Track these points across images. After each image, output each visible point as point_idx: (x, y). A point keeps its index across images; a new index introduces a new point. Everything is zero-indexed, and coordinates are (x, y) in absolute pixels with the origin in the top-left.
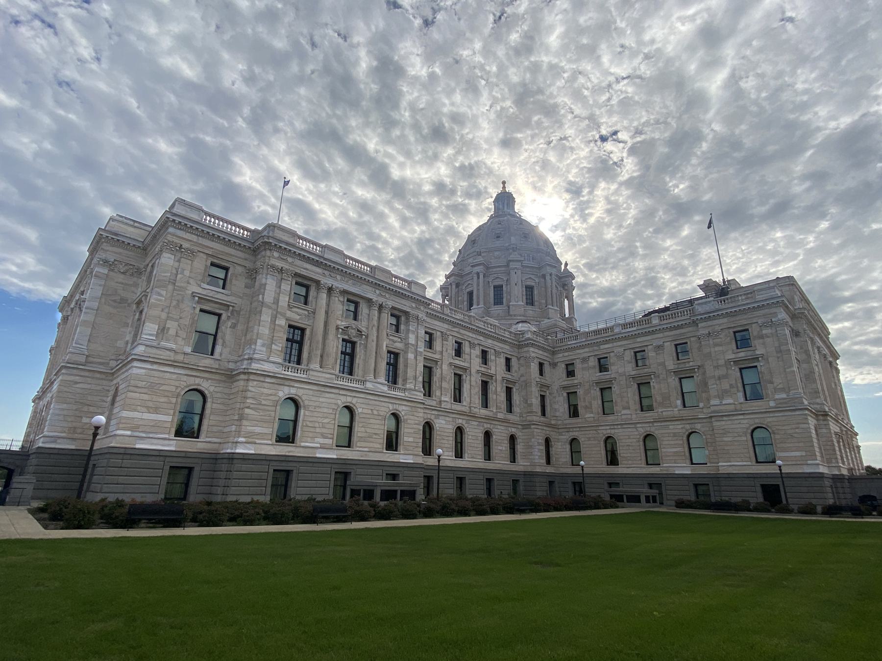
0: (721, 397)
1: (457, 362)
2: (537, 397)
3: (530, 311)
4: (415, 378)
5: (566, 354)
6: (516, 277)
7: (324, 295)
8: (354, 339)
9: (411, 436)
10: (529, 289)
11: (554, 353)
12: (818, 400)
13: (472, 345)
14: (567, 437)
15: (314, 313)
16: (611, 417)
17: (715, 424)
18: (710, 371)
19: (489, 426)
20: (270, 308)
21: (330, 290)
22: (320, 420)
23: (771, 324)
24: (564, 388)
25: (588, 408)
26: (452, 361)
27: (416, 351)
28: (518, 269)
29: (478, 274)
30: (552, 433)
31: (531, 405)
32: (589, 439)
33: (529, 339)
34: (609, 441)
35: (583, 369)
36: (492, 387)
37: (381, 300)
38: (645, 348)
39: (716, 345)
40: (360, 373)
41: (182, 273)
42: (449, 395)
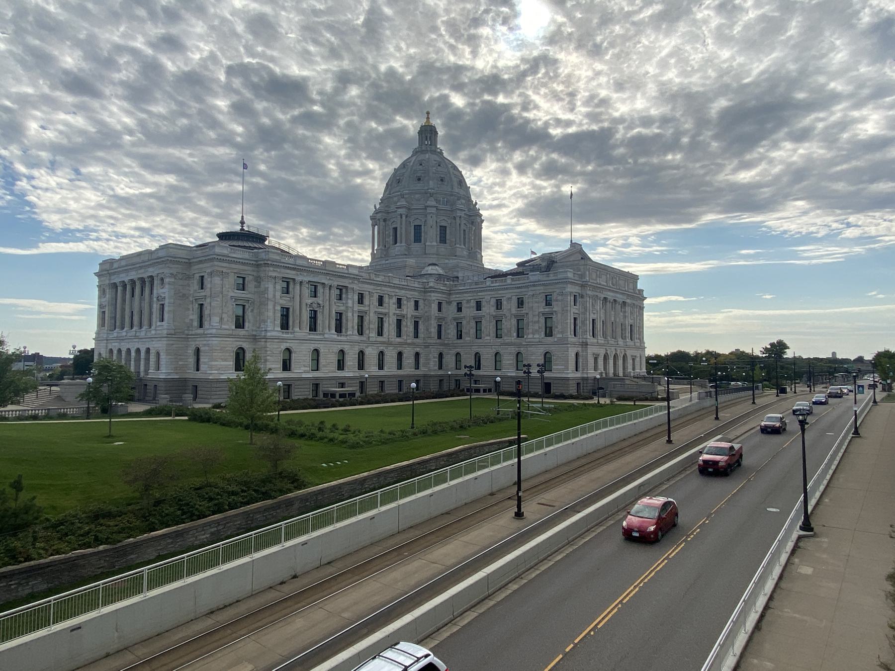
0: (534, 334)
1: (380, 310)
2: (435, 327)
3: (443, 248)
4: (353, 327)
5: (458, 296)
6: (431, 221)
7: (298, 287)
9: (351, 360)
10: (443, 229)
11: (450, 294)
12: (585, 337)
13: (390, 297)
14: (454, 352)
16: (480, 341)
18: (530, 316)
19: (401, 349)
20: (272, 301)
21: (301, 283)
22: (302, 358)
23: (562, 294)
24: (455, 319)
25: (468, 334)
26: (377, 310)
28: (433, 214)
29: (401, 215)
32: (466, 354)
33: (431, 287)
34: (478, 355)
35: (467, 307)
36: (404, 323)
39: (536, 302)
42: (374, 332)
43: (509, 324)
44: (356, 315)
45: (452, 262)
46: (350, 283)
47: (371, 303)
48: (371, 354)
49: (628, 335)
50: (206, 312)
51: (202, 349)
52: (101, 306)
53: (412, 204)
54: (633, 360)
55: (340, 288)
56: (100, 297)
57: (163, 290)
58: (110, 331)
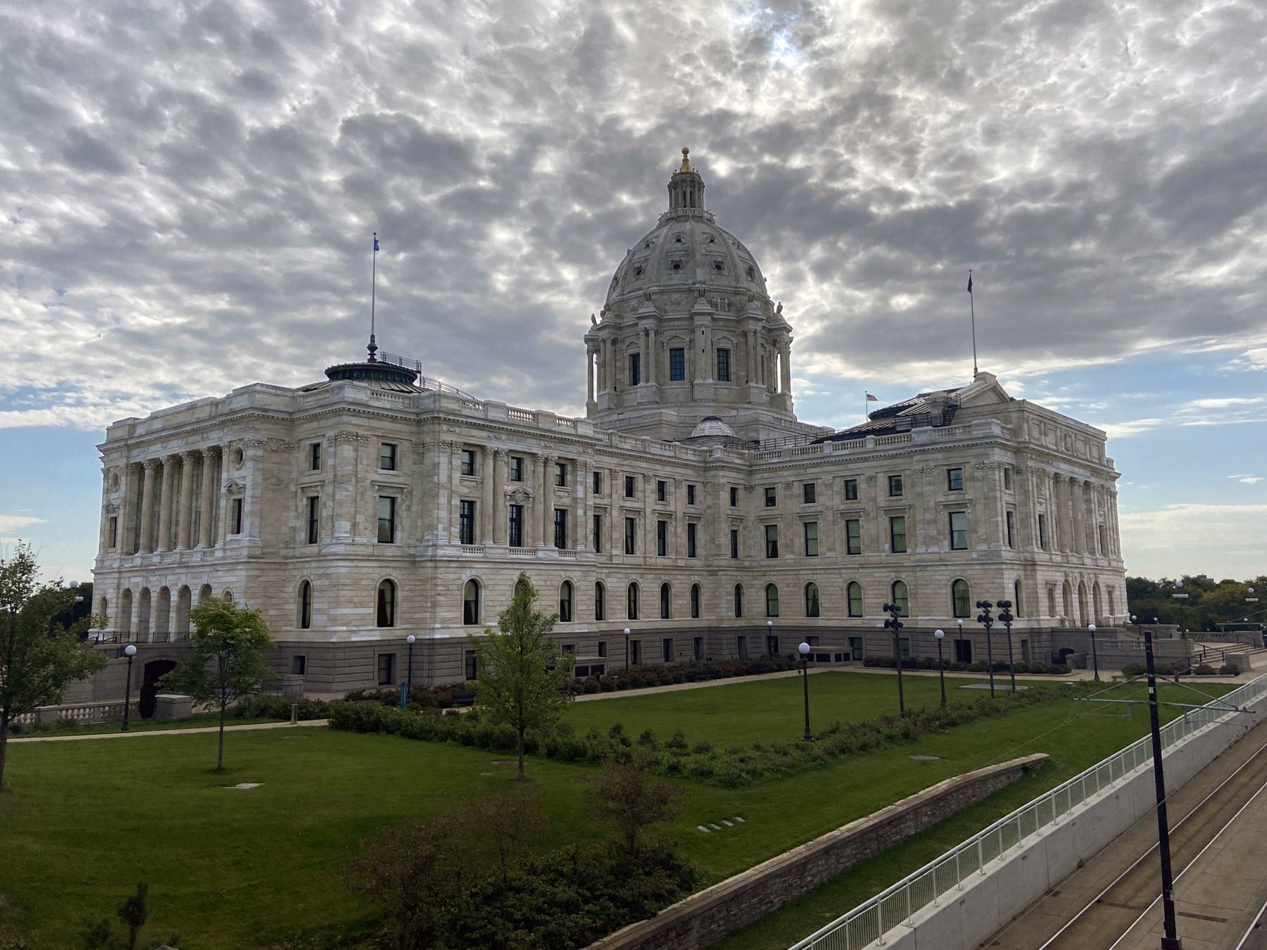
2: (726, 535)
3: (725, 390)
5: (766, 475)
6: (702, 341)
8: (521, 504)
9: (584, 603)
10: (724, 354)
11: (751, 473)
12: (1029, 548)
14: (763, 582)
15: (482, 483)
16: (815, 560)
17: (919, 574)
19: (667, 577)
20: (445, 488)
21: (496, 453)
23: (981, 467)
24: (761, 520)
27: (586, 505)
29: (647, 332)
30: (744, 578)
31: (719, 546)
32: (788, 585)
33: (718, 460)
34: (811, 587)
36: (670, 529)
37: (545, 452)
38: (857, 478)
39: (930, 484)
40: (530, 541)
41: (361, 463)
43: (874, 529)
44: (591, 514)
45: (745, 414)
46: (580, 454)
47: (614, 491)
48: (616, 586)
49: (1097, 546)
50: (324, 513)
51: (315, 583)
52: (108, 508)
53: (666, 312)
54: (1110, 593)
55: (563, 462)
56: (107, 491)
57: (243, 472)
58: (129, 554)
